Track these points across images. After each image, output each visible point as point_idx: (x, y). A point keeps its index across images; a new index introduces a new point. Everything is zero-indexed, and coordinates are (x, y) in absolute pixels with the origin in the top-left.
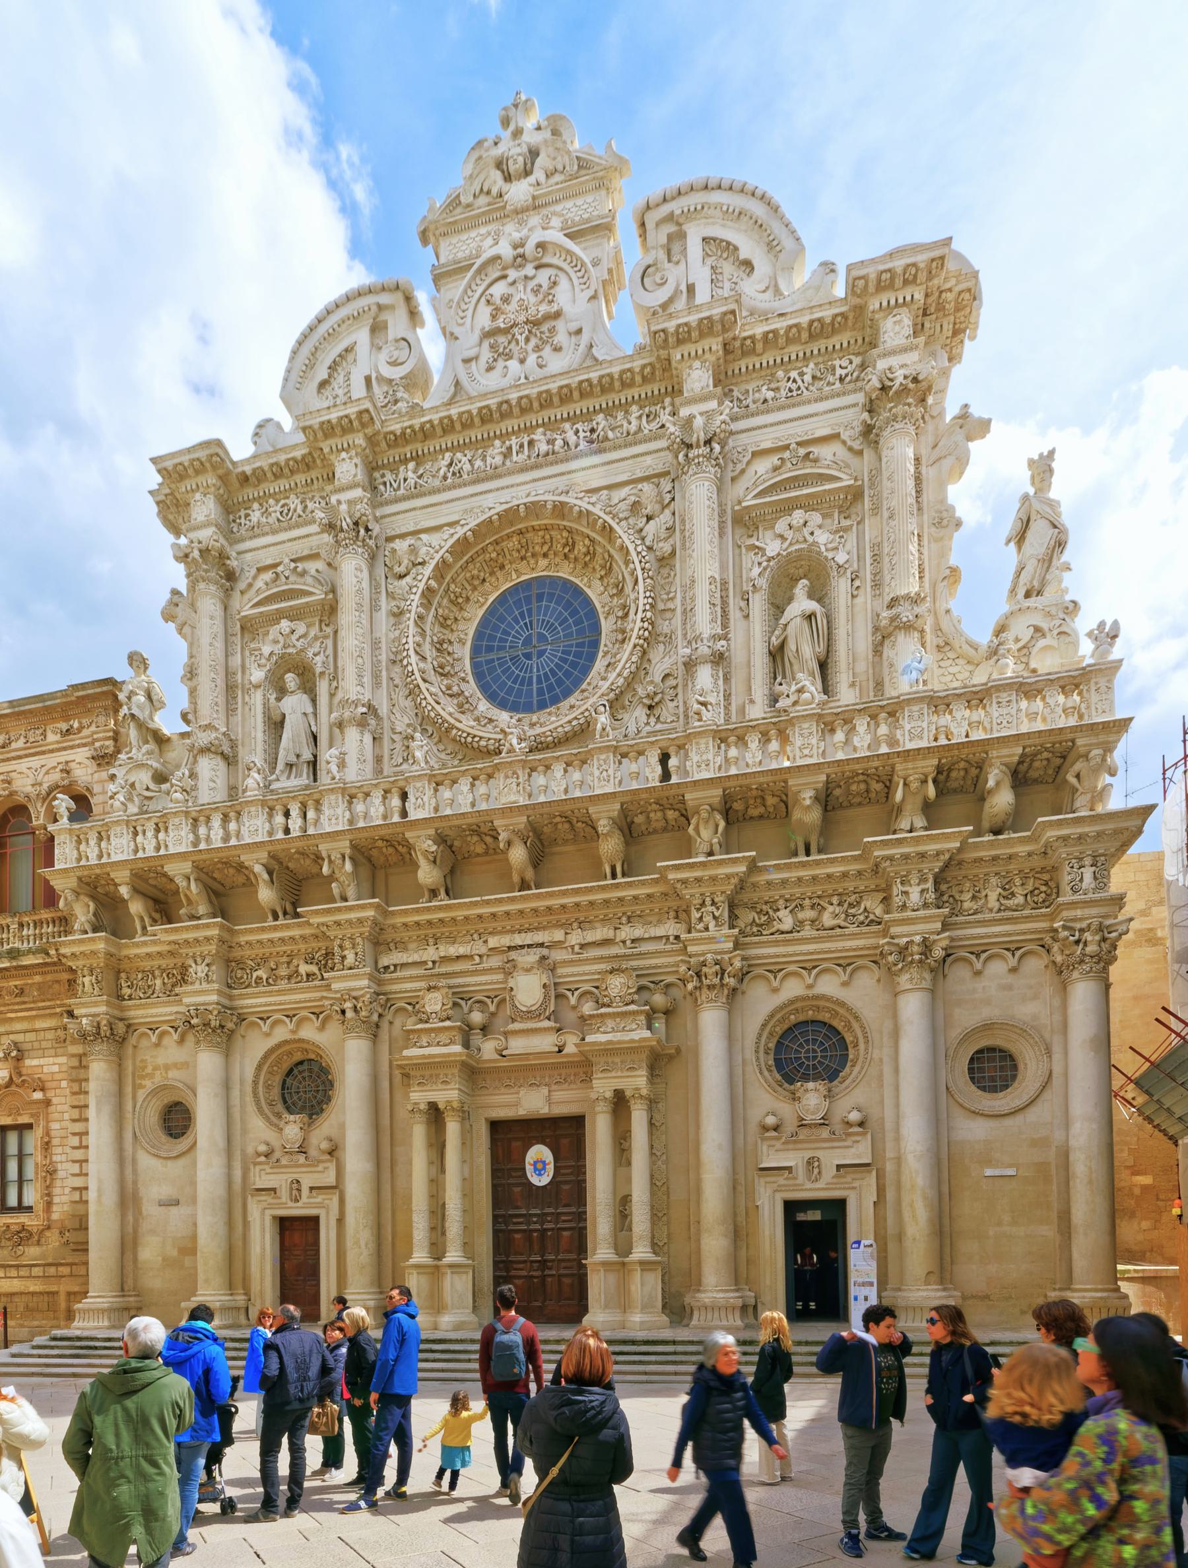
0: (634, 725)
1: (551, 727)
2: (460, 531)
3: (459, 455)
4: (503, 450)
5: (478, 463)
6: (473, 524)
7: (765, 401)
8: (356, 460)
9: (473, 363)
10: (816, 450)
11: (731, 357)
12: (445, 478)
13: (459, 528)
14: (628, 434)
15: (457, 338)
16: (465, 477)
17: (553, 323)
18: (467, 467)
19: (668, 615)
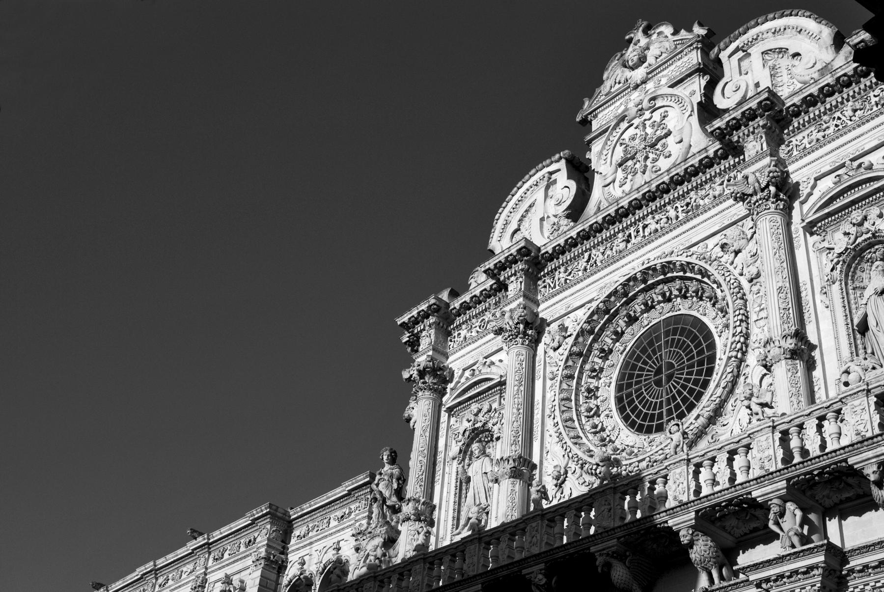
0: (738, 427)
1: (662, 446)
2: (594, 305)
3: (594, 251)
5: (608, 252)
7: (818, 140)
8: (521, 279)
9: (612, 185)
10: (866, 160)
11: (782, 123)
12: (585, 269)
13: (593, 303)
14: (715, 197)
15: (601, 173)
16: (599, 264)
17: (664, 141)
18: (601, 257)
19: (762, 323)
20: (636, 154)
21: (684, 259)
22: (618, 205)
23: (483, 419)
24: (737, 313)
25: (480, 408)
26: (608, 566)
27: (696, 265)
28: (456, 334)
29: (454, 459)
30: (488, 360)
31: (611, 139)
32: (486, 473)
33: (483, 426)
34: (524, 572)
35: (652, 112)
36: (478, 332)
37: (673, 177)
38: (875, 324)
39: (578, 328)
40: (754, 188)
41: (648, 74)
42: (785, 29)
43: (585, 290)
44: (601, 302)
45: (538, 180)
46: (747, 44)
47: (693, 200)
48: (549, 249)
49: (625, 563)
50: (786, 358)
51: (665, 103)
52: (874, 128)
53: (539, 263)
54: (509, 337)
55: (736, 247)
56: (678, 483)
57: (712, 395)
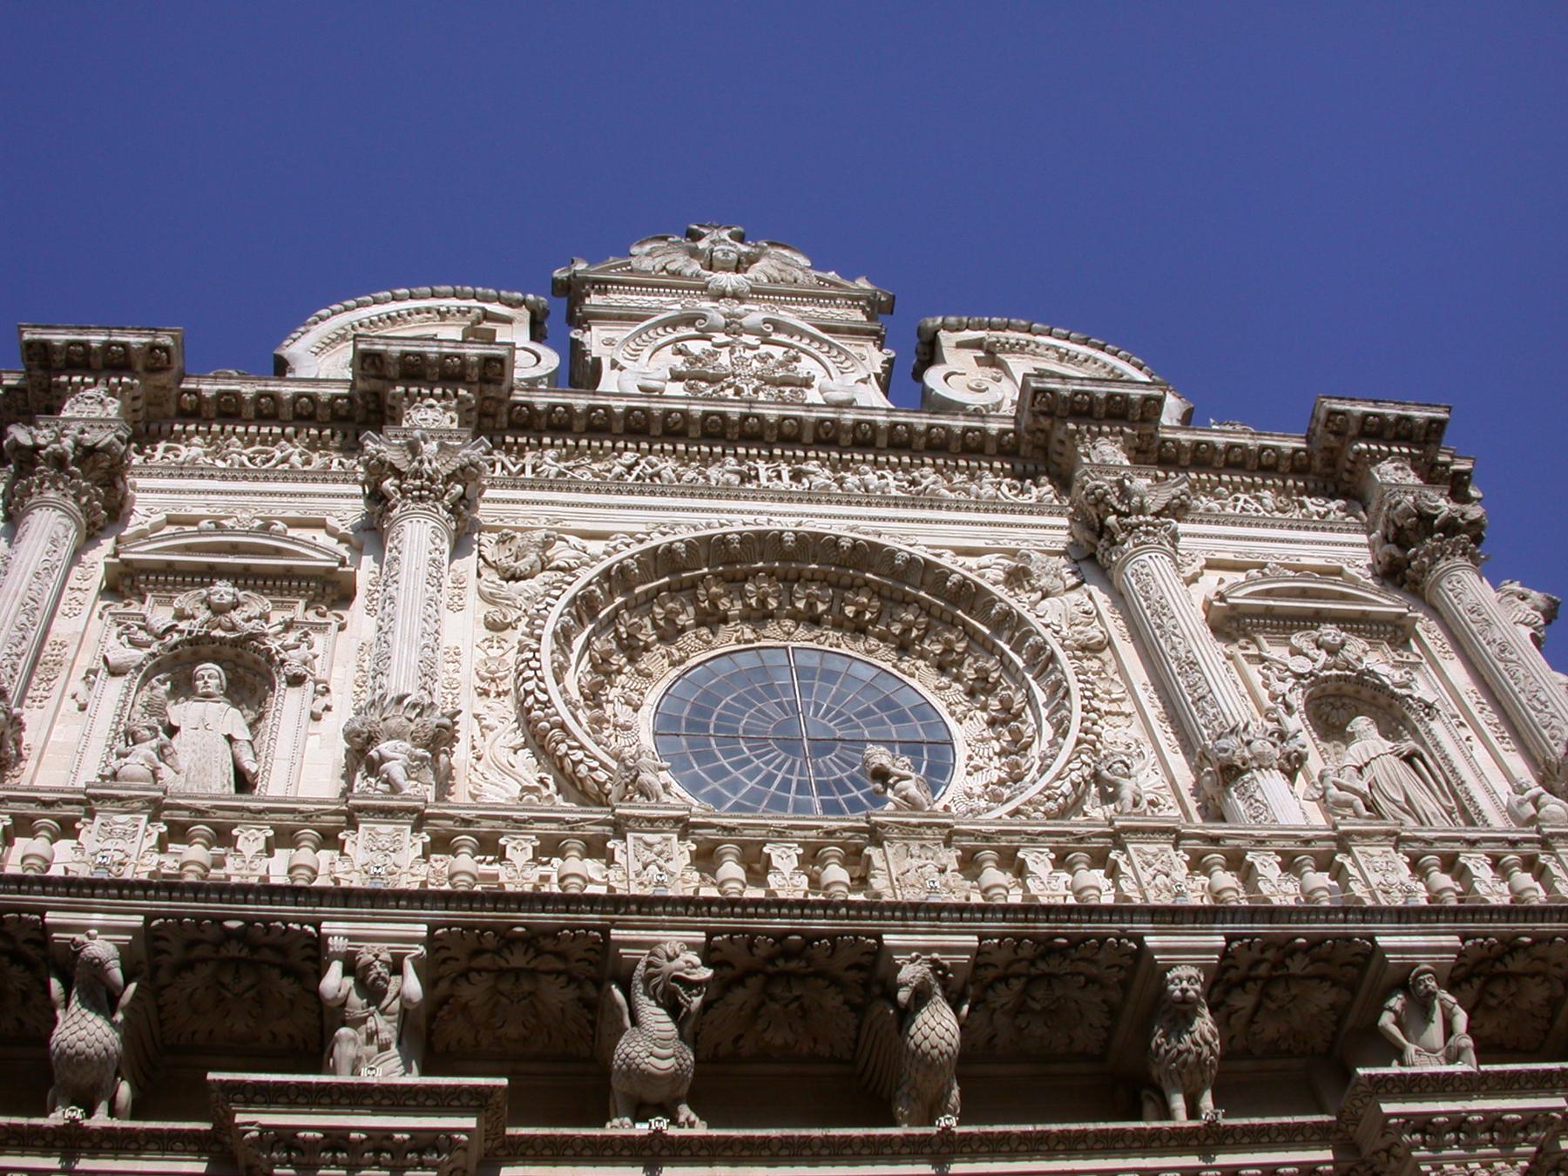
4: (745, 468)
6: (689, 535)
12: (620, 476)
15: (622, 369)
20: (727, 376)
22: (750, 408)
23: (249, 627)
24: (1081, 677)
25: (242, 599)
26: (921, 996)
27: (953, 572)
28: (161, 446)
29: (115, 672)
31: (651, 333)
32: (230, 739)
33: (235, 643)
34: (616, 934)
35: (763, 343)
36: (242, 464)
37: (896, 424)
38: (1402, 799)
39: (608, 562)
40: (1142, 502)
41: (753, 291)
42: (1086, 361)
43: (612, 511)
44: (681, 541)
45: (453, 309)
47: (925, 482)
49: (956, 1009)
50: (1282, 770)
51: (795, 341)
52: (1319, 543)
53: (494, 416)
54: (422, 488)
55: (1044, 582)
56: (1151, 871)
57: (1048, 787)
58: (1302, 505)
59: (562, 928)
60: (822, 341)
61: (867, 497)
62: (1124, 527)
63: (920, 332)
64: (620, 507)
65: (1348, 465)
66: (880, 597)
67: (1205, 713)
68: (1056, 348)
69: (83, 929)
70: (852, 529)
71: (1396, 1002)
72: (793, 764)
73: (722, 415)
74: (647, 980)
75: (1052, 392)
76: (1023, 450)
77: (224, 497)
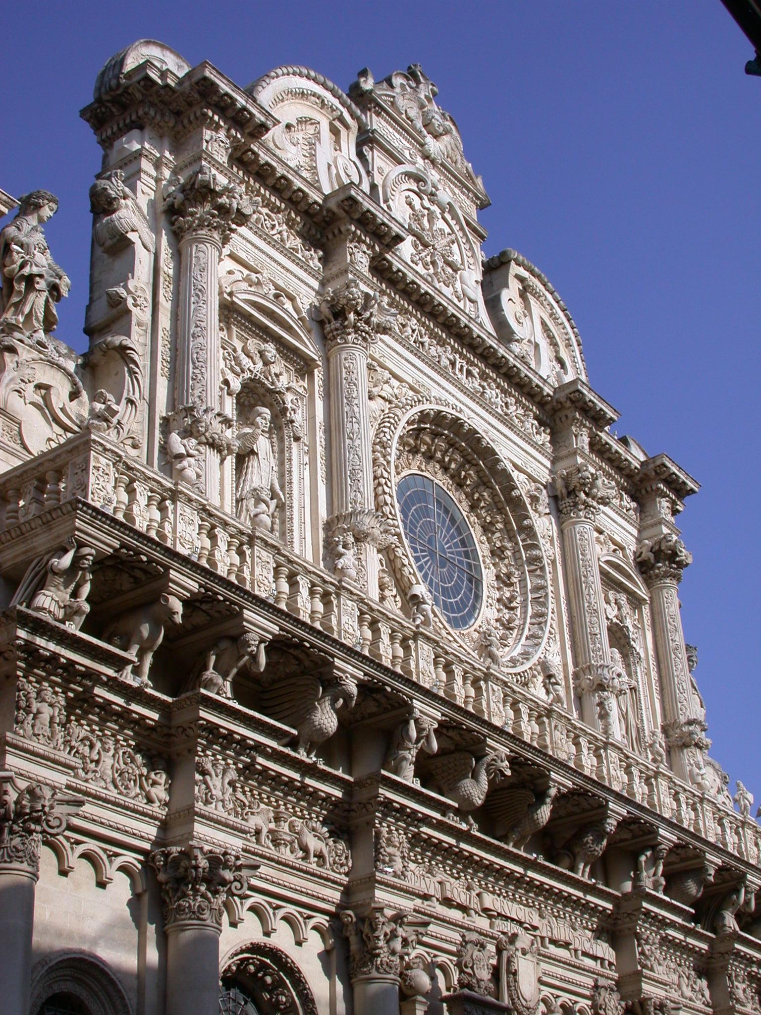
21: (510, 467)
30: (285, 300)
41: (442, 165)
43: (403, 361)
46: (536, 293)
48: (397, 265)
58: (622, 500)
59: (475, 731)
60: (465, 234)
61: (488, 407)
62: (587, 506)
63: (504, 254)
64: (406, 360)
65: (649, 489)
66: (480, 478)
67: (594, 643)
68: (552, 308)
69: (344, 672)
70: (485, 431)
71: (649, 853)
72: (428, 561)
73: (458, 319)
74: (489, 765)
75: (583, 394)
76: (548, 407)
77: (256, 251)
